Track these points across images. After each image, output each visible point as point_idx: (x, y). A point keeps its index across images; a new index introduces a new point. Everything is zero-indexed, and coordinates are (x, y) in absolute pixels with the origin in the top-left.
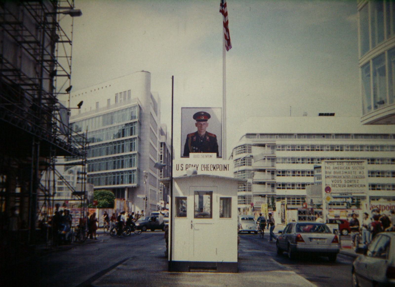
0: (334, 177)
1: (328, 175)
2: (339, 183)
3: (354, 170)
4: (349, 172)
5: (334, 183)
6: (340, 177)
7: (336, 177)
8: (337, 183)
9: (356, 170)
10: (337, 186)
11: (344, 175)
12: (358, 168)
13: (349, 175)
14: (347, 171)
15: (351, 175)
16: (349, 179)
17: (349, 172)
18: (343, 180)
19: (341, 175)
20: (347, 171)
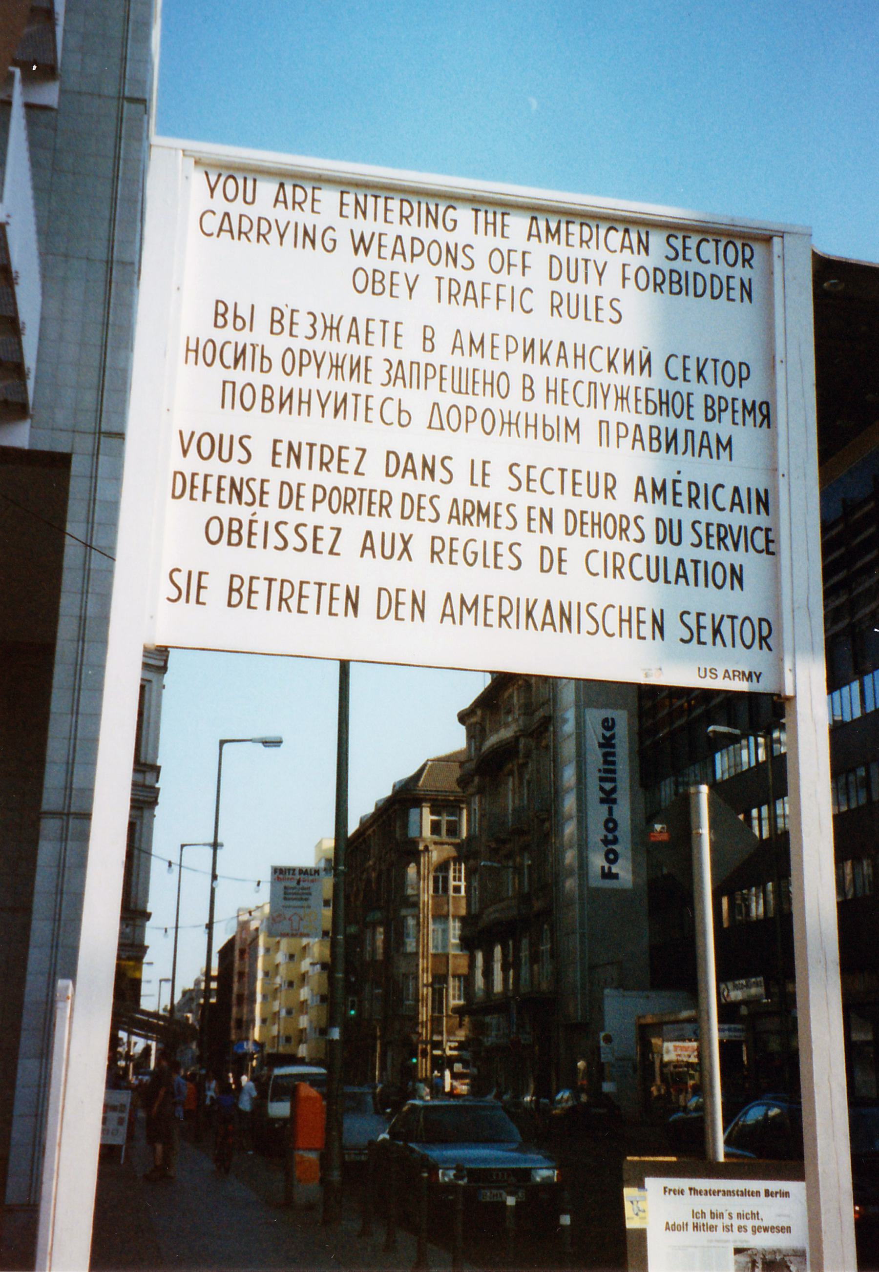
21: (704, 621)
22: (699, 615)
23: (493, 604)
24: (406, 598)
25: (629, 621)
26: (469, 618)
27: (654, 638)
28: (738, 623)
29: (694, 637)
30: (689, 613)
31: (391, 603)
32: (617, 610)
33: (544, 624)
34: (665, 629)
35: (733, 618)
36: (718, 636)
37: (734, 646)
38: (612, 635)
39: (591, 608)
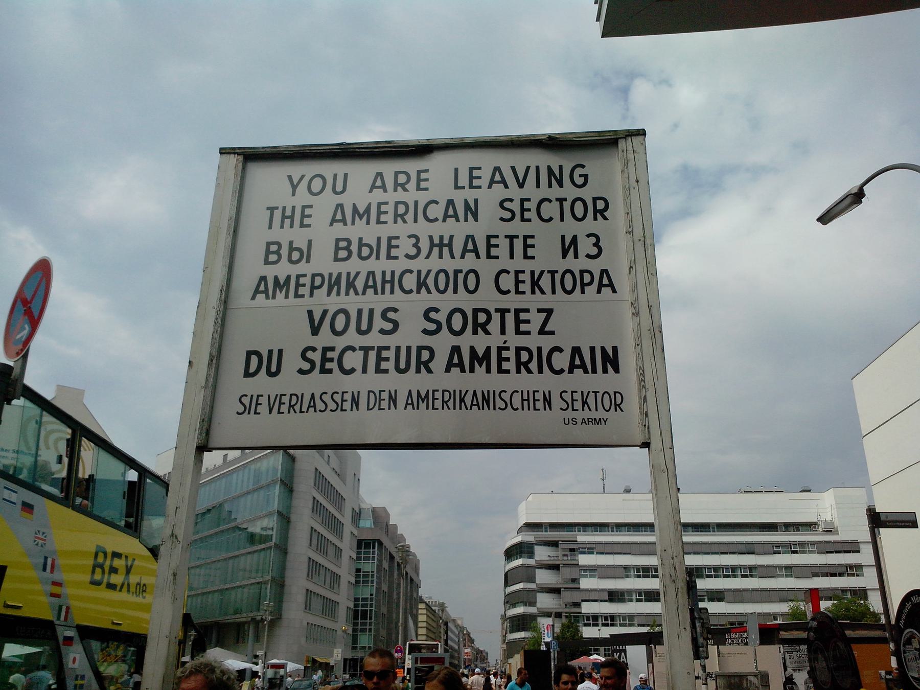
0: (334, 284)
1: (283, 269)
2: (374, 339)
3: (517, 227)
5: (325, 338)
6: (392, 282)
7: (351, 285)
8: (352, 338)
9: (534, 227)
10: (353, 360)
12: (550, 210)
13: (470, 261)
14: (458, 230)
15: (488, 269)
16: (467, 303)
19: (399, 266)
20: (458, 230)
21: (576, 396)
22: (572, 392)
23: (437, 395)
24: (385, 395)
25: (528, 400)
26: (423, 406)
29: (570, 406)
31: (377, 399)
33: (472, 405)
35: (596, 393)
38: (517, 409)
39: (503, 394)
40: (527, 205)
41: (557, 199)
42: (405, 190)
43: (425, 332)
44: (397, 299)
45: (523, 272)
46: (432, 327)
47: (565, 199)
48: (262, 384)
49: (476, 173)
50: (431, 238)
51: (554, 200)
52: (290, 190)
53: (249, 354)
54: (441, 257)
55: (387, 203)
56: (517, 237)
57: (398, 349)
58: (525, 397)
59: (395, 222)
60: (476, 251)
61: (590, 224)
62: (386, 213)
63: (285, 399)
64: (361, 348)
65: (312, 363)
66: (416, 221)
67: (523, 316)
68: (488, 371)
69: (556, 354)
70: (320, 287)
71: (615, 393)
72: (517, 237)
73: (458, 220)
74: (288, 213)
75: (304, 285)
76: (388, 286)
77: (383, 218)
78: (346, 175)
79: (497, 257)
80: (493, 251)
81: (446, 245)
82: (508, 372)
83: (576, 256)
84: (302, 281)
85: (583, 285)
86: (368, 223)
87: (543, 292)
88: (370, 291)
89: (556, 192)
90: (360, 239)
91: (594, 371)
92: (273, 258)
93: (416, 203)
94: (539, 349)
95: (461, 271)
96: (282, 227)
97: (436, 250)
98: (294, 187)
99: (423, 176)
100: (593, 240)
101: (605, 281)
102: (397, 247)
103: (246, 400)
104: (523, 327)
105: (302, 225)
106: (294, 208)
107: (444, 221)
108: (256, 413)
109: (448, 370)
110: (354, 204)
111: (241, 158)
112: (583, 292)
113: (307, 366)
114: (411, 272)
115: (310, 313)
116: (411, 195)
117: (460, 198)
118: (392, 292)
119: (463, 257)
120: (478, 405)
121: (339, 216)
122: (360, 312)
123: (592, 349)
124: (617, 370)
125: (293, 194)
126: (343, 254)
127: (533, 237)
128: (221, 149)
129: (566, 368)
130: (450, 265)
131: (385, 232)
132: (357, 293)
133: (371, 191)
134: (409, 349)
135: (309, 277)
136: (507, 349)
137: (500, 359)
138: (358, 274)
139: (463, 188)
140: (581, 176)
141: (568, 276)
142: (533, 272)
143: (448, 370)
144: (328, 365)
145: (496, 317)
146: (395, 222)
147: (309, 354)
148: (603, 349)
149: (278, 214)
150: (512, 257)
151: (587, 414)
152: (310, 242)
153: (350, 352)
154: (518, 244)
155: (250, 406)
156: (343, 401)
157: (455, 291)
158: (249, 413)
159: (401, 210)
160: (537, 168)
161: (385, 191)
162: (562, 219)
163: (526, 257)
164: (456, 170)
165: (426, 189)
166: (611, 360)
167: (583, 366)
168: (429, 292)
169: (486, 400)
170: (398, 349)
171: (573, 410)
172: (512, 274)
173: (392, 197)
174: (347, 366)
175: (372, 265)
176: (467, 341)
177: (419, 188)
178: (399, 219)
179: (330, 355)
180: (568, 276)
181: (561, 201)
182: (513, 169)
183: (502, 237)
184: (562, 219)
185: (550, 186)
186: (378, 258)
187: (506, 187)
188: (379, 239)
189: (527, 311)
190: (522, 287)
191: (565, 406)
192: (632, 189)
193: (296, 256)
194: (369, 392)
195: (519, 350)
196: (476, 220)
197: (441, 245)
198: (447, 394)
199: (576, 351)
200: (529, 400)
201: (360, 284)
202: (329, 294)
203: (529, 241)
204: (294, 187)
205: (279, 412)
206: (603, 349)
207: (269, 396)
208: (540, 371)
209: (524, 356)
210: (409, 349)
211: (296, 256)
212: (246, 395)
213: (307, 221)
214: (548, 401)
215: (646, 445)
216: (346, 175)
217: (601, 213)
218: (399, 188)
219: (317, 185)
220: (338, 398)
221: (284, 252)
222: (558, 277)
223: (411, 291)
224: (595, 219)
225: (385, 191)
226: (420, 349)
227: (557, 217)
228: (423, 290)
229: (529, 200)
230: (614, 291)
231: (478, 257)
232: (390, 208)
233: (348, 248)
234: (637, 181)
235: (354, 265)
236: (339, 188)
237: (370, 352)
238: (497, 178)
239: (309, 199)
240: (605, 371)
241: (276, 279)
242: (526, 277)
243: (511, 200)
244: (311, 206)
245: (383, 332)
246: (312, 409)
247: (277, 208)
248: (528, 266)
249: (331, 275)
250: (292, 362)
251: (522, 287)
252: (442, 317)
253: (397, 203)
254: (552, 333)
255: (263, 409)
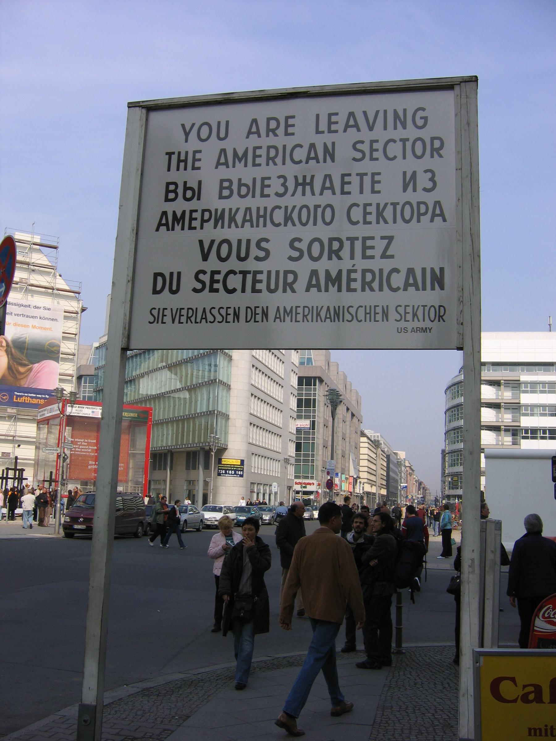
0: (219, 219)
1: (180, 206)
2: (251, 265)
3: (367, 166)
4: (328, 177)
5: (213, 263)
6: (264, 217)
7: (232, 219)
8: (233, 264)
9: (381, 165)
10: (234, 282)
11: (298, 200)
12: (395, 149)
13: (327, 198)
16: (324, 233)
17: (328, 177)
18: (279, 239)
20: (318, 171)
23: (300, 310)
24: (259, 311)
25: (370, 313)
26: (288, 319)
27: (383, 321)
28: (427, 309)
29: (403, 318)
30: (400, 306)
32: (364, 308)
33: (326, 318)
34: (389, 315)
35: (424, 306)
36: (416, 317)
37: (424, 321)
38: (361, 321)
39: (350, 309)
40: (375, 146)
41: (401, 140)
42: (276, 135)
43: (291, 258)
44: (268, 231)
45: (370, 205)
46: (296, 254)
47: (408, 140)
48: (166, 300)
49: (334, 119)
50: (296, 177)
51: (398, 141)
52: (184, 137)
53: (156, 275)
54: (304, 194)
55: (260, 148)
56: (366, 174)
57: (269, 273)
58: (368, 311)
59: (268, 164)
60: (332, 188)
61: (427, 162)
62: (260, 156)
63: (184, 312)
64: (241, 272)
65: (203, 283)
66: (284, 163)
67: (369, 243)
68: (339, 290)
69: (394, 275)
70: (208, 221)
71: (440, 306)
72: (366, 174)
73: (318, 162)
74: (183, 157)
75: (196, 219)
76: (261, 220)
77: (258, 161)
78: (227, 122)
79: (349, 193)
80: (347, 188)
81: (308, 184)
82: (355, 290)
83: (415, 190)
84: (194, 215)
85: (420, 215)
86: (246, 166)
87: (386, 222)
88: (247, 224)
89: (400, 133)
90: (240, 180)
91: (424, 289)
92: (171, 196)
93: (284, 147)
94: (381, 271)
95: (319, 206)
96: (178, 169)
97: (300, 188)
98: (187, 134)
99: (291, 122)
100: (429, 175)
101: (438, 211)
102: (269, 186)
103: (155, 312)
104: (369, 252)
105: (194, 168)
106: (187, 153)
107: (307, 162)
108: (163, 323)
109: (307, 290)
110: (235, 149)
111: (144, 111)
112: (419, 221)
113: (199, 286)
114: (280, 208)
115: (201, 242)
116: (280, 140)
117: (319, 141)
118: (265, 225)
119: (321, 194)
120: (330, 318)
121: (222, 160)
122: (240, 241)
123: (424, 270)
124: (442, 288)
125: (186, 141)
126: (226, 193)
127: (379, 174)
128: (129, 103)
129: (402, 287)
130: (311, 200)
131: (259, 173)
132: (237, 226)
133: (247, 137)
134: (277, 272)
135: (200, 212)
136: (355, 271)
137: (350, 280)
138: (238, 209)
139: (323, 132)
140: (421, 118)
141: (407, 209)
142: (378, 205)
143: (307, 290)
144: (216, 286)
145: (347, 244)
146: (268, 164)
147: (201, 276)
148: (432, 269)
149: (174, 158)
150: (361, 192)
151: (417, 324)
152: (200, 183)
153: (232, 275)
154: (367, 180)
155: (158, 317)
156: (227, 314)
157: (315, 224)
158: (158, 323)
159: (272, 153)
160: (385, 112)
161: (259, 136)
162: (404, 158)
163: (373, 191)
164: (318, 116)
165: (293, 134)
166: (438, 280)
167: (415, 285)
168: (294, 225)
169: (337, 314)
170: (269, 273)
171: (405, 321)
172: (361, 207)
173: (265, 141)
174: (230, 287)
175: (249, 202)
176: (323, 266)
177: (287, 134)
178: (270, 161)
179: (217, 277)
180: (407, 209)
181: (404, 141)
182: (365, 113)
183: (354, 175)
184: (404, 158)
185: (395, 128)
186: (253, 196)
187: (359, 130)
188: (254, 179)
189: (372, 238)
190: (369, 218)
191: (399, 318)
192: (463, 131)
193: (189, 194)
194: (247, 308)
195: (364, 272)
196: (333, 161)
197: (304, 184)
198: (306, 309)
199: (411, 271)
200: (371, 314)
201: (239, 218)
202: (215, 227)
203: (377, 178)
204: (187, 134)
205: (180, 323)
206: (432, 269)
207: (172, 309)
208: (381, 289)
209: (369, 277)
210: (277, 272)
211: (189, 194)
212: (155, 309)
213: (197, 164)
214: (385, 314)
215: (460, 349)
216: (227, 122)
217: (436, 152)
218: (271, 134)
219: (205, 132)
220: (223, 312)
221: (180, 190)
222: (399, 208)
223: (279, 225)
224: (432, 156)
225: (259, 136)
226: (286, 273)
227: (400, 155)
228: (289, 223)
229: (377, 141)
230: (444, 220)
231: (334, 193)
232: (262, 152)
233: (229, 188)
234: (468, 124)
235: (235, 202)
236: (222, 135)
237: (248, 275)
238: (352, 122)
239: (199, 145)
240: (433, 288)
241: (174, 213)
242: (372, 209)
243: (362, 142)
244: (200, 152)
245: (257, 259)
246: (204, 321)
247: (174, 153)
248: (374, 199)
249: (216, 210)
250: (188, 282)
251: (369, 218)
252: (303, 246)
253: (269, 148)
254: (392, 257)
255: (168, 319)
